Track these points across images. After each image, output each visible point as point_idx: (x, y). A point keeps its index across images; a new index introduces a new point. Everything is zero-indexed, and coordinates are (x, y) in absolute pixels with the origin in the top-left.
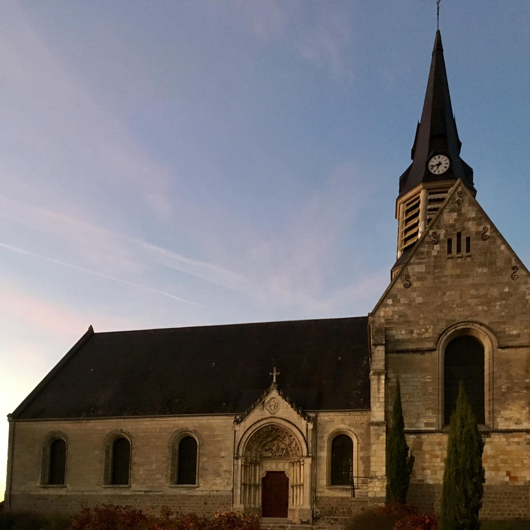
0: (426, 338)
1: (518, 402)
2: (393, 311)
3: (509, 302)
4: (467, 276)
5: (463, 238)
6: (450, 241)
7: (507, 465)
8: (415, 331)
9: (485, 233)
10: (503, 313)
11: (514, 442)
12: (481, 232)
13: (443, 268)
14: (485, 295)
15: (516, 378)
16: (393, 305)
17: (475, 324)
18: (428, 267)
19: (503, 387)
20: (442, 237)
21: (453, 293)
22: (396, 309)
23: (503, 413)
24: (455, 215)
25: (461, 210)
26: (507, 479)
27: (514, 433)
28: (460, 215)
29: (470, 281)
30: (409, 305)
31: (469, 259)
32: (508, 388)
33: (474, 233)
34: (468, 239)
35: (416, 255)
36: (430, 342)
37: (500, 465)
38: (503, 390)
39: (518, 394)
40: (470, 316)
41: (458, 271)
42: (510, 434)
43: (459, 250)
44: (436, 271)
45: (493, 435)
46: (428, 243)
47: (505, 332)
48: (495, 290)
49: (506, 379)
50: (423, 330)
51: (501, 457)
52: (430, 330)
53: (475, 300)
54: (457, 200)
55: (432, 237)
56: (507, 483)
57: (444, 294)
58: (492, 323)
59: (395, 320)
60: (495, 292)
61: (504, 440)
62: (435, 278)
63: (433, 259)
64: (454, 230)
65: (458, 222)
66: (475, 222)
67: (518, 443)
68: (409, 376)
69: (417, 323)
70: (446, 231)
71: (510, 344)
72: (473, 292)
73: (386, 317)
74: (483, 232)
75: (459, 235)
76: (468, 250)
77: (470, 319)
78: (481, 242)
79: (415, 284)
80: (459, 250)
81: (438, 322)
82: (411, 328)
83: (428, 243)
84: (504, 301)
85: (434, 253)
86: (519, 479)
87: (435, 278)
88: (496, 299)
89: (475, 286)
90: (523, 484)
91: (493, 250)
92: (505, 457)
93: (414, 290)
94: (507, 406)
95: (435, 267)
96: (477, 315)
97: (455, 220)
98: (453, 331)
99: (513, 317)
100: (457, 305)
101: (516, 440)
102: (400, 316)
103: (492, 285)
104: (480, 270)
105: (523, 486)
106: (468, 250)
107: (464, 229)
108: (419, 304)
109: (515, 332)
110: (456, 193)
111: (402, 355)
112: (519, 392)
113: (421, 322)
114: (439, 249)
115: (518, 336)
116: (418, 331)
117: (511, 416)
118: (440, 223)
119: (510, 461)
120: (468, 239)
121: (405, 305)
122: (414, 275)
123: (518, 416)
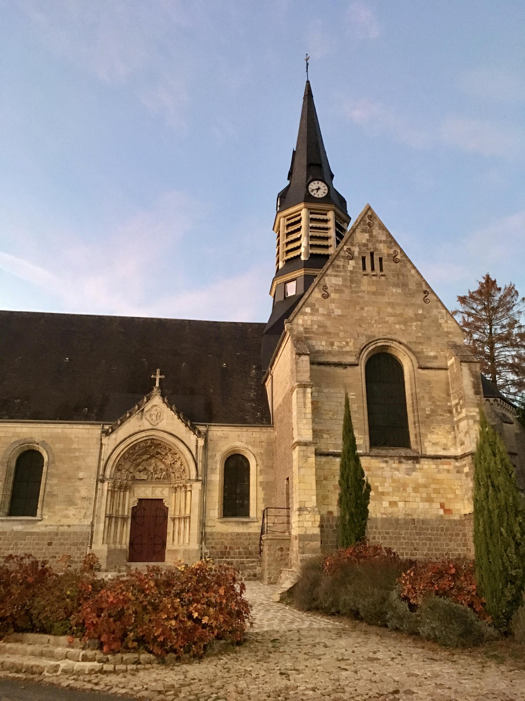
0: (347, 352)
1: (443, 425)
2: (312, 321)
3: (424, 323)
4: (383, 294)
5: (376, 258)
6: (364, 259)
7: (440, 496)
8: (336, 344)
9: (396, 256)
10: (420, 334)
11: (444, 470)
12: (392, 254)
13: (359, 283)
14: (401, 315)
15: (438, 401)
16: (311, 314)
17: (394, 342)
18: (345, 280)
19: (427, 409)
20: (356, 254)
21: (371, 308)
22: (315, 318)
23: (429, 436)
24: (367, 236)
25: (372, 232)
26: (441, 512)
27: (443, 460)
28: (371, 236)
29: (386, 299)
30: (329, 315)
31: (383, 278)
32: (432, 411)
33: (386, 255)
34: (381, 260)
35: (333, 268)
36: (352, 356)
37: (434, 496)
38: (427, 413)
39: (442, 417)
40: (389, 334)
41: (374, 288)
42: (439, 460)
43: (373, 269)
44: (353, 286)
45: (422, 461)
46: (343, 257)
47: (423, 352)
48: (410, 311)
49: (429, 401)
50: (344, 343)
51: (433, 486)
52: (351, 344)
53: (392, 319)
54: (367, 222)
55: (347, 253)
56: (442, 516)
57: (362, 309)
58: (410, 342)
59: (314, 330)
60: (410, 312)
61: (434, 466)
62: (352, 292)
63: (349, 274)
64: (368, 249)
65: (370, 242)
66: (386, 245)
67: (448, 471)
68: (332, 391)
69: (337, 335)
70: (360, 249)
71: (429, 365)
72: (390, 310)
73: (305, 326)
74: (394, 255)
75: (372, 254)
76: (381, 270)
77: (389, 336)
78: (393, 264)
79: (333, 296)
80: (373, 269)
81: (358, 336)
82: (331, 340)
83: (343, 257)
84: (419, 323)
85: (350, 268)
86: (454, 512)
87: (352, 292)
88: (412, 320)
89: (392, 305)
90: (459, 518)
91: (405, 273)
92: (437, 486)
93: (333, 301)
94: (433, 430)
95: (352, 281)
96: (396, 334)
97: (368, 240)
98: (373, 347)
99: (429, 338)
100: (376, 321)
101: (446, 467)
102: (319, 326)
103: (406, 305)
104: (394, 290)
105: (459, 521)
106: (381, 270)
107: (376, 249)
108: (339, 316)
109: (432, 354)
110: (367, 216)
111: (323, 368)
112: (443, 416)
113: (341, 334)
114: (354, 265)
115: (435, 357)
116: (339, 344)
117: (438, 440)
118: (353, 240)
119: (442, 491)
120: (381, 260)
121: (323, 315)
122: (331, 286)
123: (445, 441)
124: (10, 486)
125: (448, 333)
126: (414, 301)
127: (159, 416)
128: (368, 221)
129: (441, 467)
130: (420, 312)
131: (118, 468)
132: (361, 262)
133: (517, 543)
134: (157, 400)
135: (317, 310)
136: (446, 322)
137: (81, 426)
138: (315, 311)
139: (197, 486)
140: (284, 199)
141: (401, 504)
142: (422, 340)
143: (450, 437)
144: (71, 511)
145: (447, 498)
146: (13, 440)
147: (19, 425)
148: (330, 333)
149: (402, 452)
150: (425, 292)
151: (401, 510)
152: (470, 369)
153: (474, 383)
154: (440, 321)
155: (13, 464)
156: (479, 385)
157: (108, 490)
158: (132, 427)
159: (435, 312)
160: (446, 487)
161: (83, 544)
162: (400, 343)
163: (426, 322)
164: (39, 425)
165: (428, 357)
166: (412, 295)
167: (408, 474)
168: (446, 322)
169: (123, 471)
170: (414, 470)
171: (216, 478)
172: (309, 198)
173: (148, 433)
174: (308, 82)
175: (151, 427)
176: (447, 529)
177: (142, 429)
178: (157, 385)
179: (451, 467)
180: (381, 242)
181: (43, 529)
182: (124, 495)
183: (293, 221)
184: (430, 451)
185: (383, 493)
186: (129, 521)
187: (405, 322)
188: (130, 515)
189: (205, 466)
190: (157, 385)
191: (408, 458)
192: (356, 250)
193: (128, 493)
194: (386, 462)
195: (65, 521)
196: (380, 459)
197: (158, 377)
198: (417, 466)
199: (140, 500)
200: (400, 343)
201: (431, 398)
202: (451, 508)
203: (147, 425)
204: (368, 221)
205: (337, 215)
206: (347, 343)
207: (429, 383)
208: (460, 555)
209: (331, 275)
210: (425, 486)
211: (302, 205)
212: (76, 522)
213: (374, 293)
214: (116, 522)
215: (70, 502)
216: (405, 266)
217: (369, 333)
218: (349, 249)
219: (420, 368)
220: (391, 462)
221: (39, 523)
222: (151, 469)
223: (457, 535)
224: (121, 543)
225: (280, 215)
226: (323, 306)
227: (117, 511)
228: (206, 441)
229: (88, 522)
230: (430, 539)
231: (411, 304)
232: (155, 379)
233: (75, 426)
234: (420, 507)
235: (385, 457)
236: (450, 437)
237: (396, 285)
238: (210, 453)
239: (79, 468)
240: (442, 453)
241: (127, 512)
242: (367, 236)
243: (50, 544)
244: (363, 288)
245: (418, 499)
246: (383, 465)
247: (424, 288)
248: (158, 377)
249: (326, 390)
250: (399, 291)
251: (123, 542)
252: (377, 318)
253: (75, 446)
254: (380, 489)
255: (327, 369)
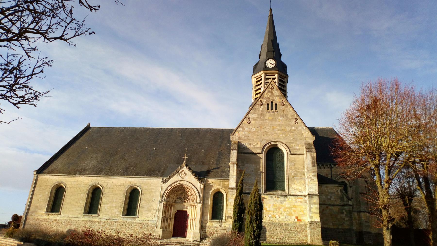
2: (242, 134)
4: (276, 121)
5: (274, 104)
6: (268, 105)
7: (296, 213)
13: (264, 116)
14: (283, 130)
18: (258, 115)
20: (264, 103)
21: (269, 127)
22: (243, 133)
23: (293, 186)
24: (270, 94)
26: (296, 220)
27: (299, 197)
28: (272, 94)
29: (276, 123)
30: (250, 131)
32: (295, 174)
34: (276, 105)
37: (293, 213)
41: (271, 118)
43: (272, 109)
46: (258, 104)
47: (293, 147)
51: (293, 209)
52: (259, 144)
53: (279, 132)
57: (265, 128)
58: (287, 143)
60: (288, 128)
63: (260, 112)
67: (301, 202)
68: (249, 165)
69: (253, 140)
72: (278, 128)
75: (272, 102)
76: (276, 109)
77: (277, 140)
78: (281, 106)
79: (252, 122)
80: (272, 109)
83: (258, 104)
85: (261, 109)
87: (261, 120)
88: (289, 132)
89: (280, 125)
92: (295, 209)
93: (252, 125)
95: (261, 115)
97: (270, 96)
99: (296, 140)
101: (300, 200)
103: (286, 125)
106: (276, 109)
107: (274, 100)
109: (297, 148)
111: (246, 155)
113: (255, 140)
115: (299, 149)
116: (253, 144)
119: (297, 211)
120: (276, 105)
121: (248, 131)
123: (300, 188)
124: (127, 203)
125: (306, 138)
126: (290, 123)
127: (185, 174)
128: (271, 87)
129: (297, 200)
130: (293, 128)
131: (168, 197)
132: (266, 106)
133: (254, 230)
134: (185, 169)
135: (245, 129)
136: (305, 132)
137: (154, 179)
138: (243, 129)
139: (200, 205)
140: (256, 69)
141: (277, 216)
142: (293, 141)
143: (303, 186)
144: (149, 215)
145: (299, 214)
146: (129, 184)
147: (130, 178)
148: (250, 139)
149: (280, 192)
150: (296, 119)
151: (276, 220)
152: (311, 155)
153: (312, 162)
154: (302, 132)
155: (128, 194)
156: (314, 162)
157: (163, 206)
158: (175, 179)
159: (300, 128)
160: (299, 209)
161: (154, 228)
162: (282, 143)
163: (296, 133)
164: (138, 178)
165: (295, 149)
166: (290, 120)
167: (281, 203)
168: (305, 132)
169: (170, 198)
170: (284, 201)
171: (210, 201)
172: (266, 68)
173: (180, 182)
174: (271, 8)
175: (181, 179)
176: (298, 229)
177: (178, 180)
178: (185, 161)
179: (302, 200)
180: (276, 96)
181: (138, 221)
182: (171, 209)
183: (258, 80)
184: (293, 193)
185: (269, 211)
186: (173, 220)
187: (286, 133)
188: (173, 217)
189: (204, 196)
190: (185, 161)
191: (282, 195)
192: (264, 102)
193: (173, 208)
194: (272, 197)
195: (147, 219)
196: (269, 196)
197: (185, 158)
198: (286, 199)
199: (178, 211)
200: (282, 143)
201: (295, 168)
202: (301, 219)
203: (180, 179)
204: (271, 87)
205: (280, 76)
206: (257, 144)
207: (295, 161)
208: (303, 240)
209: (252, 113)
210: (289, 208)
211: (262, 72)
212: (151, 219)
213: (271, 120)
214: (167, 220)
215: (149, 210)
216: (287, 107)
217: (267, 139)
218: (261, 101)
219: (291, 154)
220: (274, 197)
221: (137, 219)
222: (182, 197)
223: (303, 231)
224: (169, 228)
225: (253, 77)
226: (248, 127)
227: (168, 215)
228: (204, 186)
229: (156, 219)
230: (290, 232)
231: (289, 125)
232: (184, 159)
233: (152, 179)
234: (286, 218)
235: (271, 195)
236: (303, 186)
237: (283, 116)
238: (206, 191)
239: (153, 196)
240: (298, 193)
241: (172, 215)
242: (270, 94)
243: (141, 228)
244: (266, 118)
245: (285, 214)
246: (270, 198)
247: (296, 117)
248: (185, 158)
249: (246, 165)
250: (283, 119)
251: (170, 228)
252: (272, 132)
253: (152, 187)
254: (268, 209)
255: (247, 155)
